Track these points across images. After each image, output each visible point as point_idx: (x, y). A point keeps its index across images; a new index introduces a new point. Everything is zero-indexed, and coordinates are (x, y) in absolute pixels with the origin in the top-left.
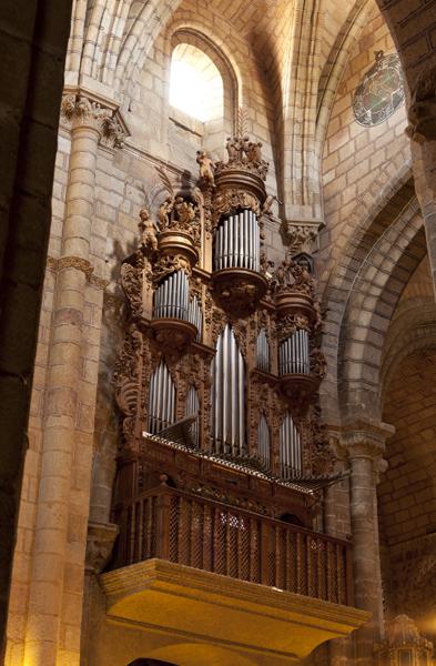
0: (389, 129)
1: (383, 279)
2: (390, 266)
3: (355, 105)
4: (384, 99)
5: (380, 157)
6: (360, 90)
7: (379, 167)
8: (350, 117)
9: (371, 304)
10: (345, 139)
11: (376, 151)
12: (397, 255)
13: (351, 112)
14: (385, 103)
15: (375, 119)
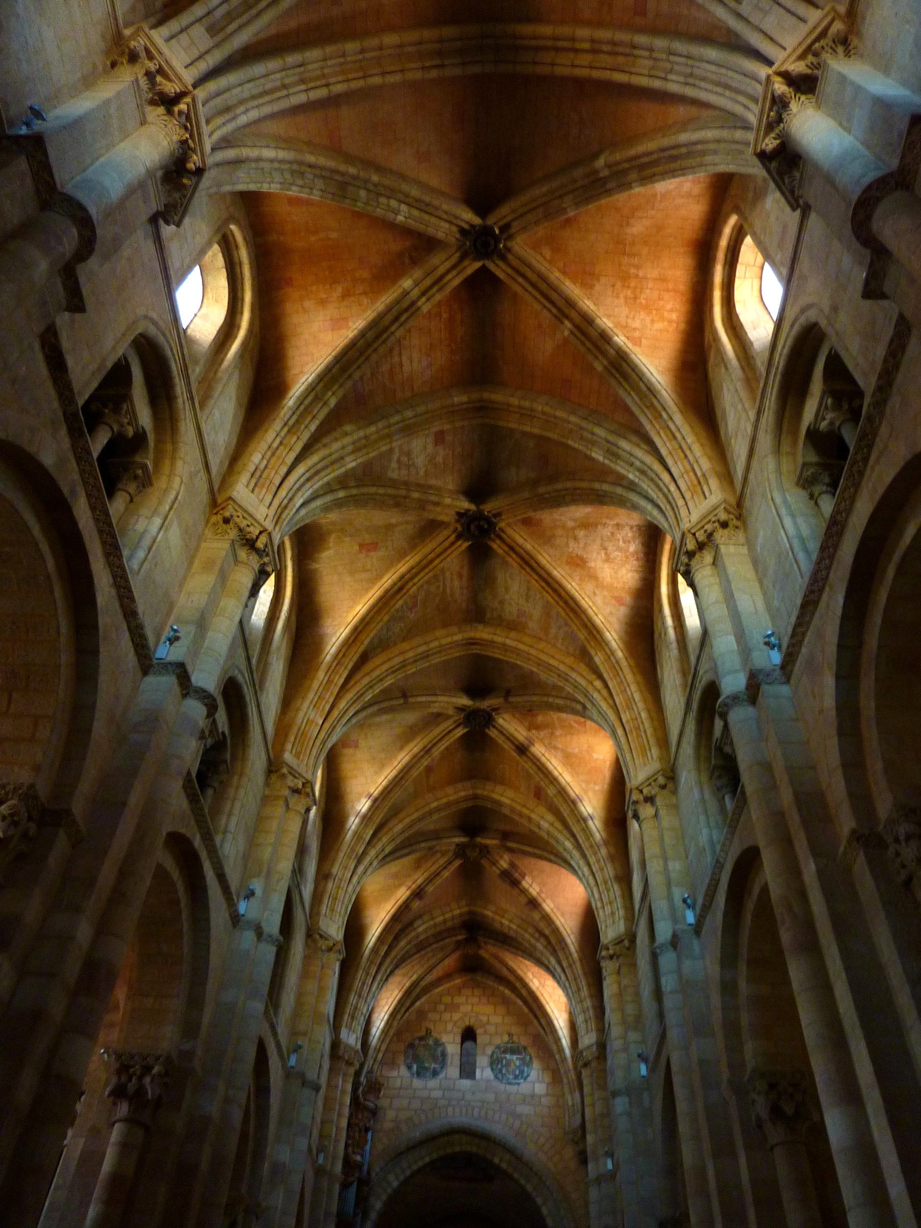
0: (426, 1088)
1: (395, 1184)
2: (402, 1178)
3: (405, 1053)
4: (427, 1065)
5: (416, 1104)
6: (411, 1046)
7: (416, 1111)
8: (401, 1059)
9: (384, 1197)
10: (394, 1073)
11: (414, 1097)
12: (408, 1173)
13: (402, 1058)
14: (427, 1069)
15: (419, 1074)
